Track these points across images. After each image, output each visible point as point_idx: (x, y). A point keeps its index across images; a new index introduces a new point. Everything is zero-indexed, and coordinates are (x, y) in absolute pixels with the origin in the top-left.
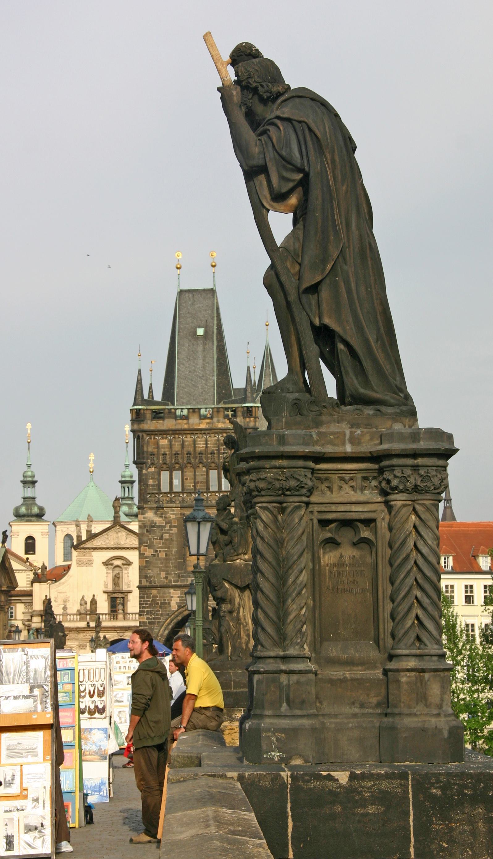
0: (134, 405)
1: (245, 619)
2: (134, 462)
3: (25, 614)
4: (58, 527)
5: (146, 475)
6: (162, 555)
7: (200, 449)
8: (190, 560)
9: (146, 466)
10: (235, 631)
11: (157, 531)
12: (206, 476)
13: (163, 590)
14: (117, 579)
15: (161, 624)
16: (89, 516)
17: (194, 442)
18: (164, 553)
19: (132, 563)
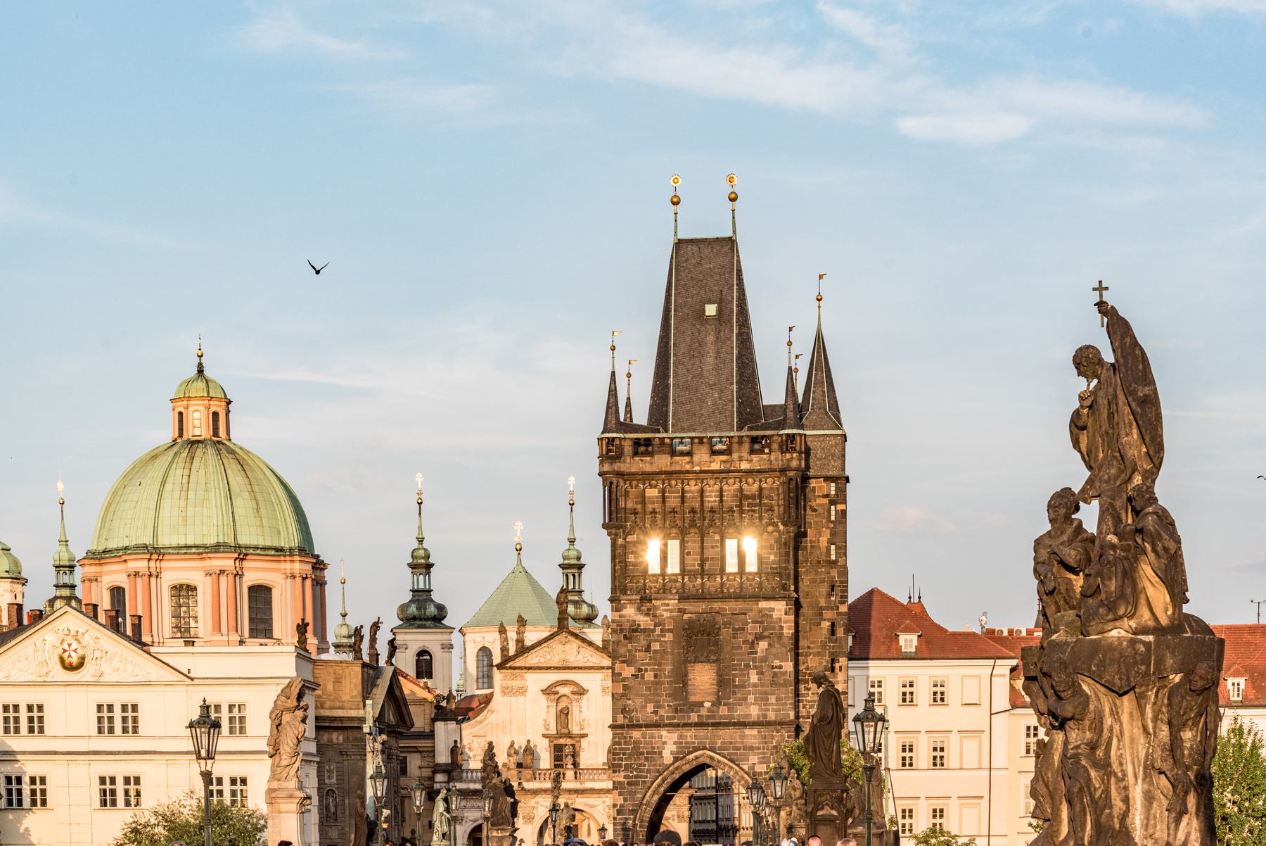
0: (603, 433)
1: (1121, 764)
2: (605, 526)
3: (423, 770)
4: (468, 637)
5: (624, 547)
6: (649, 676)
7: (710, 505)
8: (694, 685)
9: (624, 532)
10: (1100, 790)
11: (642, 638)
12: (719, 549)
13: (650, 732)
14: (563, 715)
15: (648, 784)
16: (520, 617)
17: (702, 492)
19: (588, 691)
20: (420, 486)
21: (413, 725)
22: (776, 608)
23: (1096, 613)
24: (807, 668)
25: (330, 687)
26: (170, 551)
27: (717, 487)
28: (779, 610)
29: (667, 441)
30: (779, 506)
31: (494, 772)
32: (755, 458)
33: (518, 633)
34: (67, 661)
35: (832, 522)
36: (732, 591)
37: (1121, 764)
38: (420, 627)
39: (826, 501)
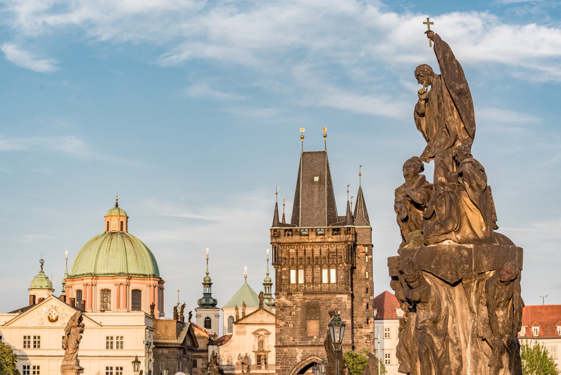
0: (272, 227)
1: (455, 334)
2: (273, 264)
3: (203, 365)
6: (291, 325)
9: (281, 267)
11: (288, 310)
12: (320, 274)
14: (261, 343)
15: (290, 371)
18: (292, 324)
20: (207, 253)
21: (198, 347)
22: (344, 297)
23: (433, 229)
24: (357, 323)
25: (163, 331)
26: (101, 275)
27: (319, 249)
28: (345, 298)
29: (298, 230)
30: (344, 256)
31: (215, 364)
32: (334, 237)
33: (243, 310)
34: (51, 318)
35: (367, 263)
36: (325, 290)
37: (455, 334)
38: (206, 308)
39: (364, 254)
